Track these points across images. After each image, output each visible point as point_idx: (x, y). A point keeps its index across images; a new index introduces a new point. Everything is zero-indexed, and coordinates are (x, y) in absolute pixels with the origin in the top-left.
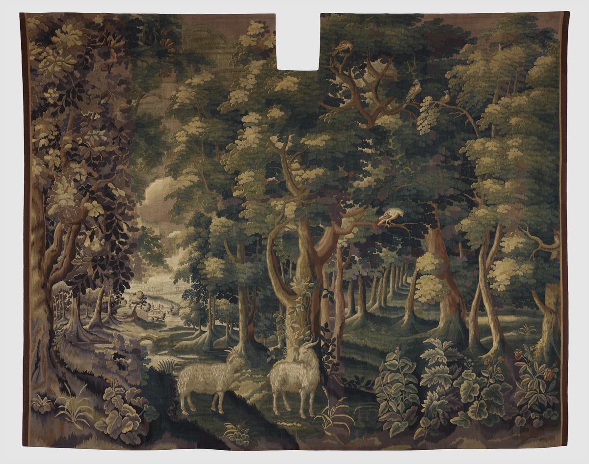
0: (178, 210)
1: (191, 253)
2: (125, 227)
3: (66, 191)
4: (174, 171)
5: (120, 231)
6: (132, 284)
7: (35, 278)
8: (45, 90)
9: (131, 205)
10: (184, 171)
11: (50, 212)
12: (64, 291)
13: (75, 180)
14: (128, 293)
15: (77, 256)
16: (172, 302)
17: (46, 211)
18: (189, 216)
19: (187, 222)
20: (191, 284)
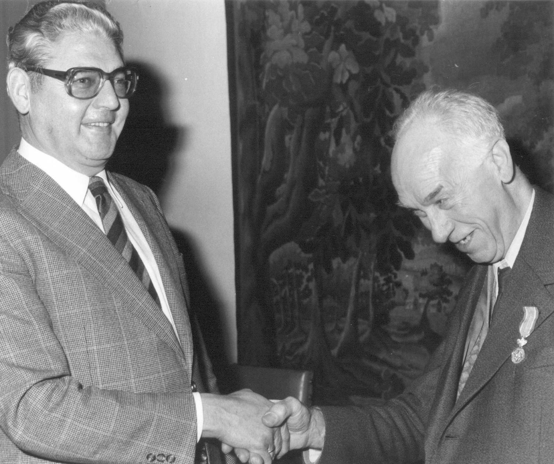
3: (287, 30)
5: (388, 113)
9: (409, 42)
12: (298, 266)
14: (409, 271)
15: (321, 182)
17: (259, 83)
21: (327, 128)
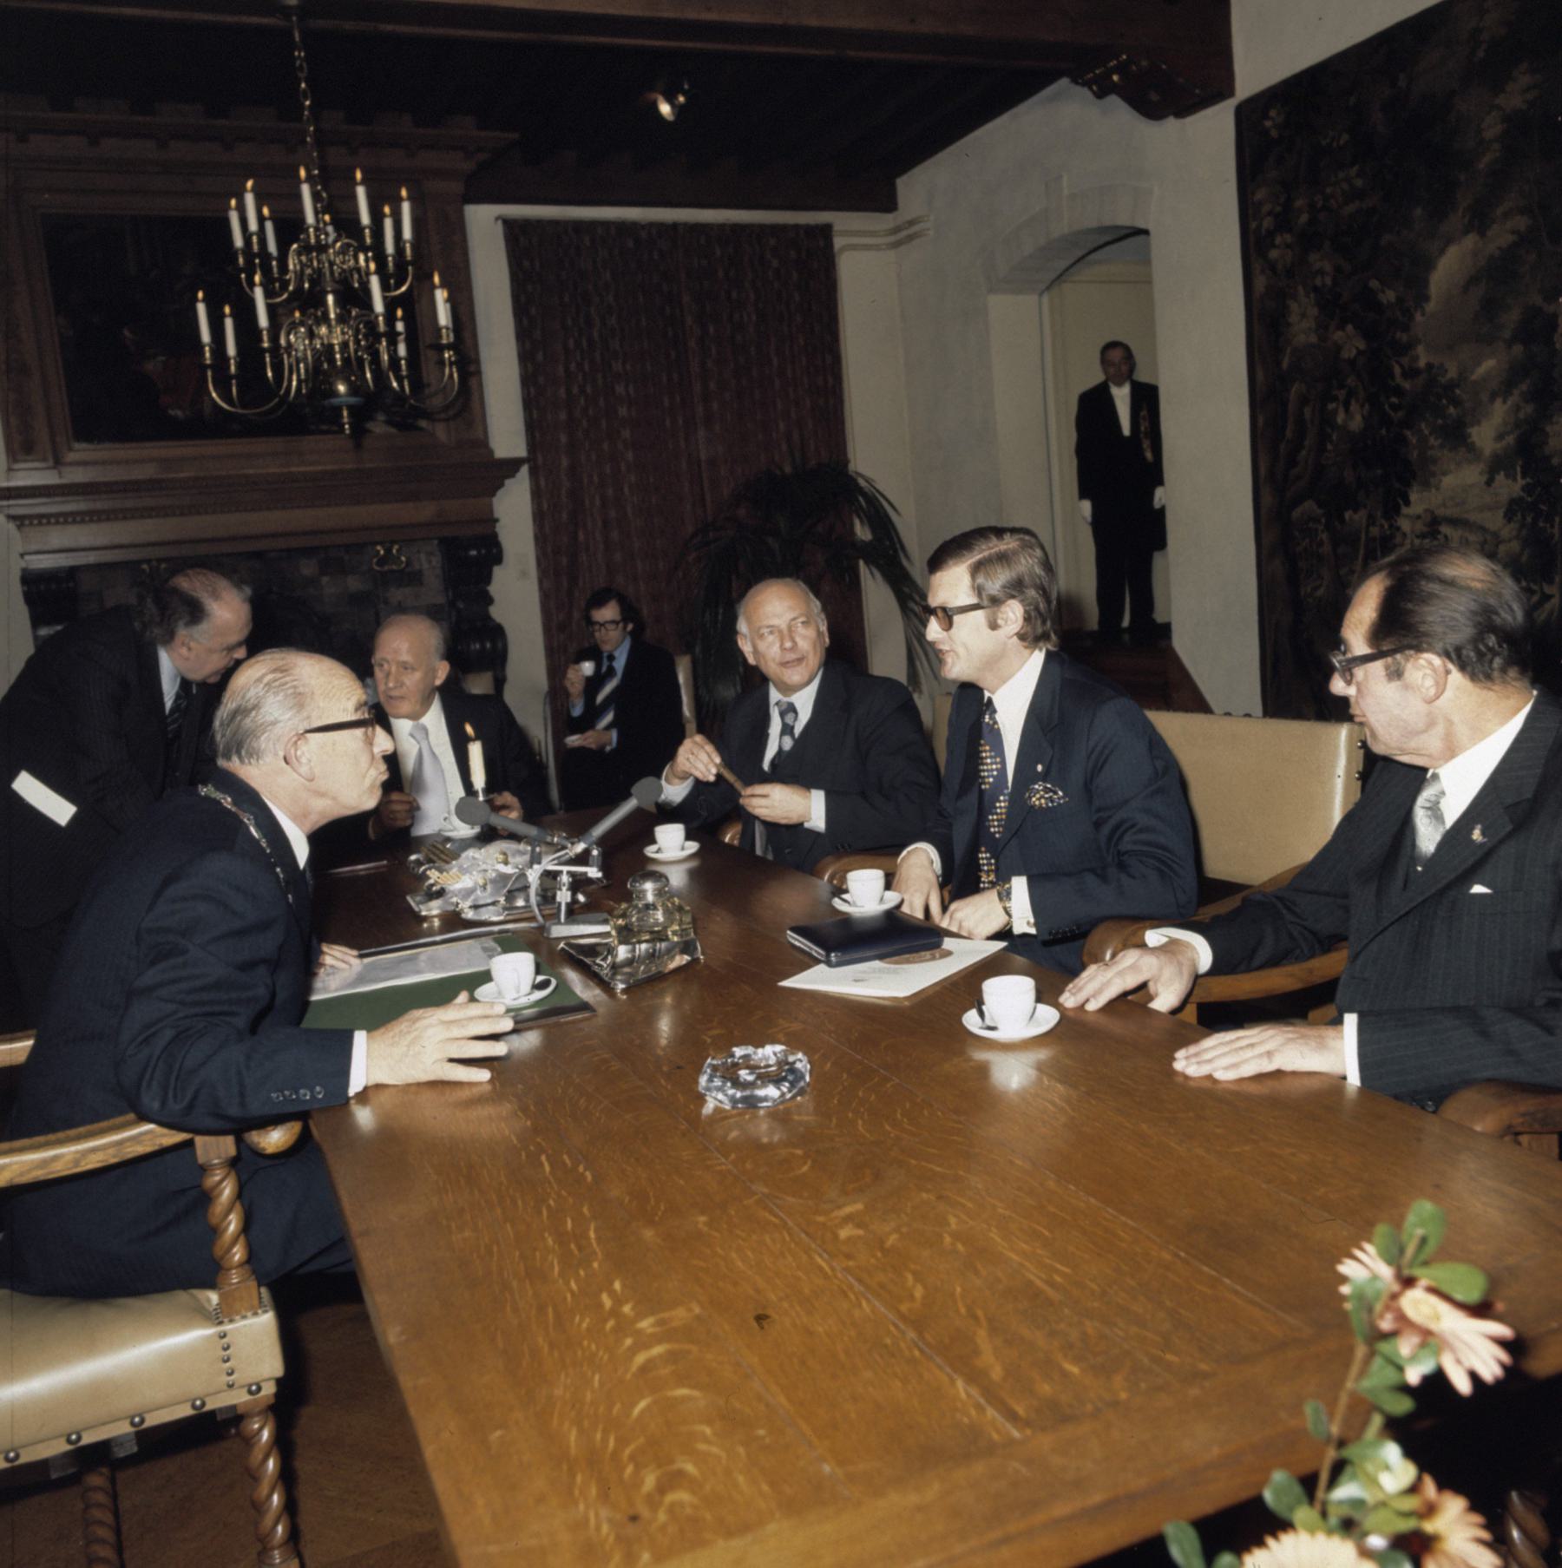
0: (1491, 307)
1: (1518, 408)
2: (1397, 370)
3: (1303, 315)
4: (1479, 221)
6: (1413, 497)
7: (1267, 500)
8: (1266, 116)
10: (1499, 211)
11: (1285, 365)
13: (1315, 289)
14: (1407, 516)
16: (1483, 529)
18: (1511, 318)
19: (1507, 334)
20: (1521, 482)
21: (1335, 399)
